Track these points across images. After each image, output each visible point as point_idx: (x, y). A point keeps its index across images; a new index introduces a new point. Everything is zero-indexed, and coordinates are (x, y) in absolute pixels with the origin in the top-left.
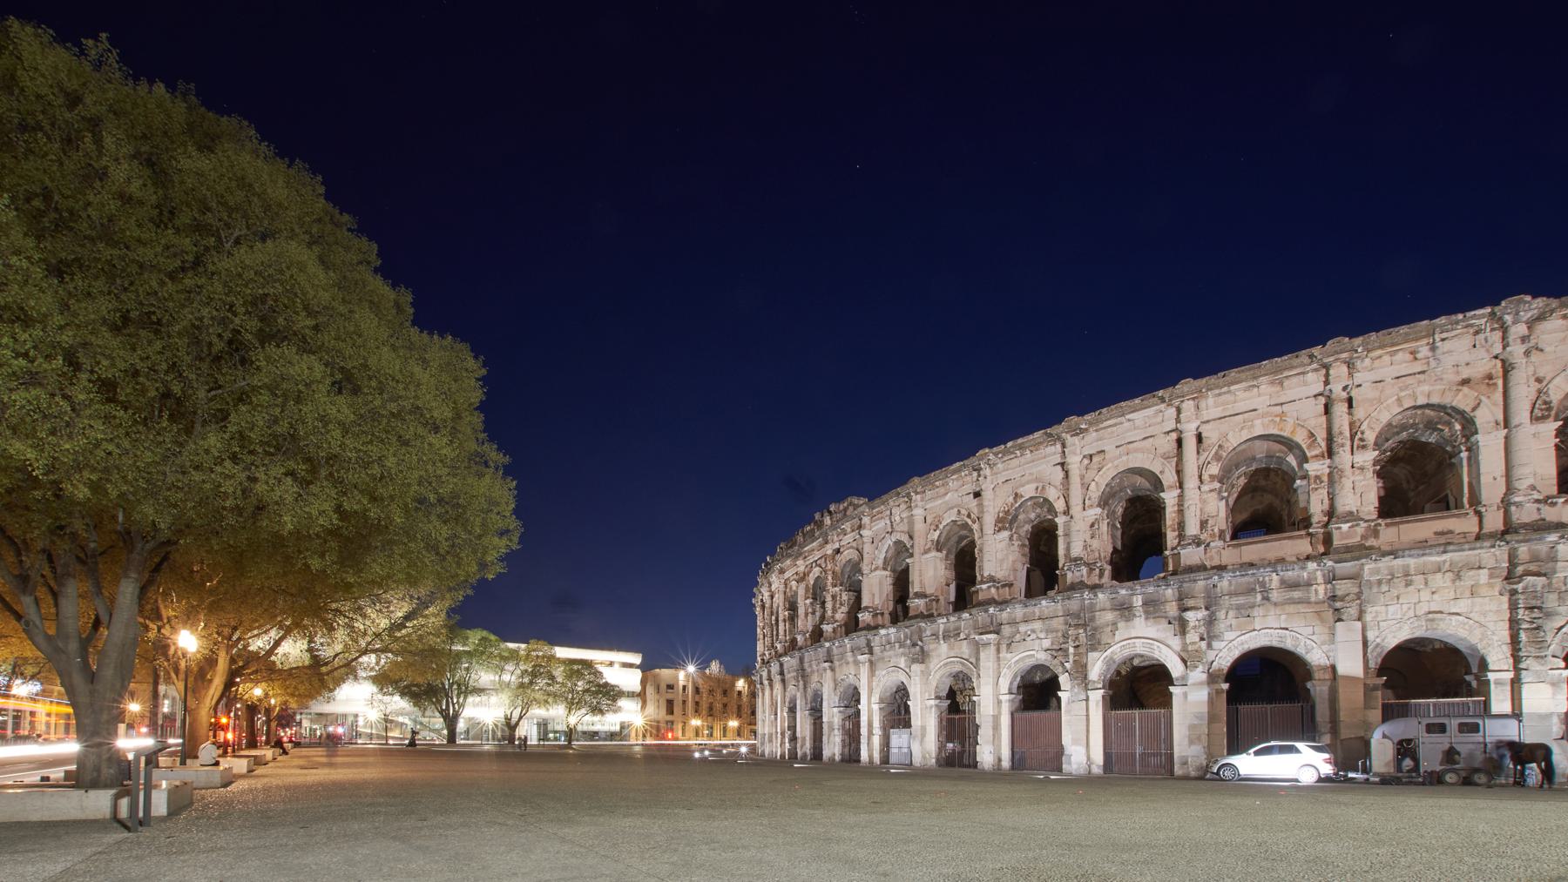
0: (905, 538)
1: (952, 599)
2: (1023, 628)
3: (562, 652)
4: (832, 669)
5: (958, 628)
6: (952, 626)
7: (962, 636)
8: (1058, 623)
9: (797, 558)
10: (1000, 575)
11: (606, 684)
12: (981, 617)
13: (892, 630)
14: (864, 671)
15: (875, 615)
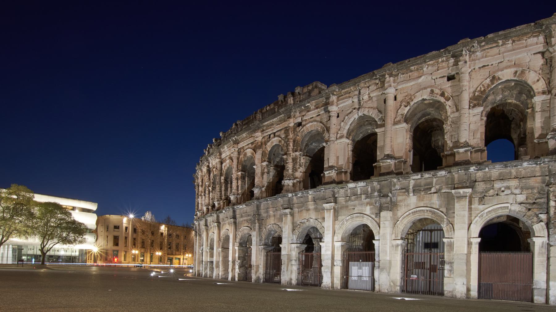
0: (373, 114)
1: (411, 164)
2: (497, 185)
3: (40, 198)
4: (292, 215)
5: (431, 183)
6: (423, 182)
7: (433, 190)
8: (536, 182)
9: (255, 131)
10: (473, 142)
11: (74, 222)
12: (458, 174)
13: (361, 184)
14: (329, 216)
15: (339, 173)
